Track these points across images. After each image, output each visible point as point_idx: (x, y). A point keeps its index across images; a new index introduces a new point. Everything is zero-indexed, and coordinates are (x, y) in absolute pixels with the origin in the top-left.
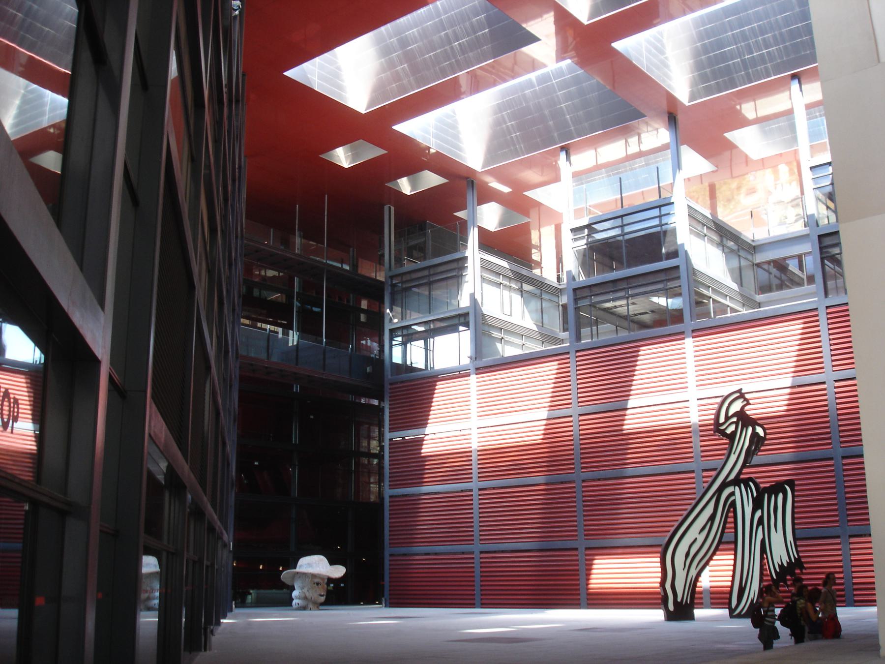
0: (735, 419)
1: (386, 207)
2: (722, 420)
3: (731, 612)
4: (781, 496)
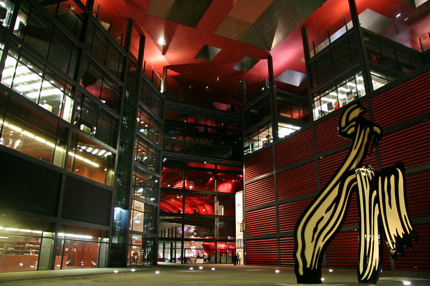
0: (354, 123)
2: (343, 124)
4: (393, 177)
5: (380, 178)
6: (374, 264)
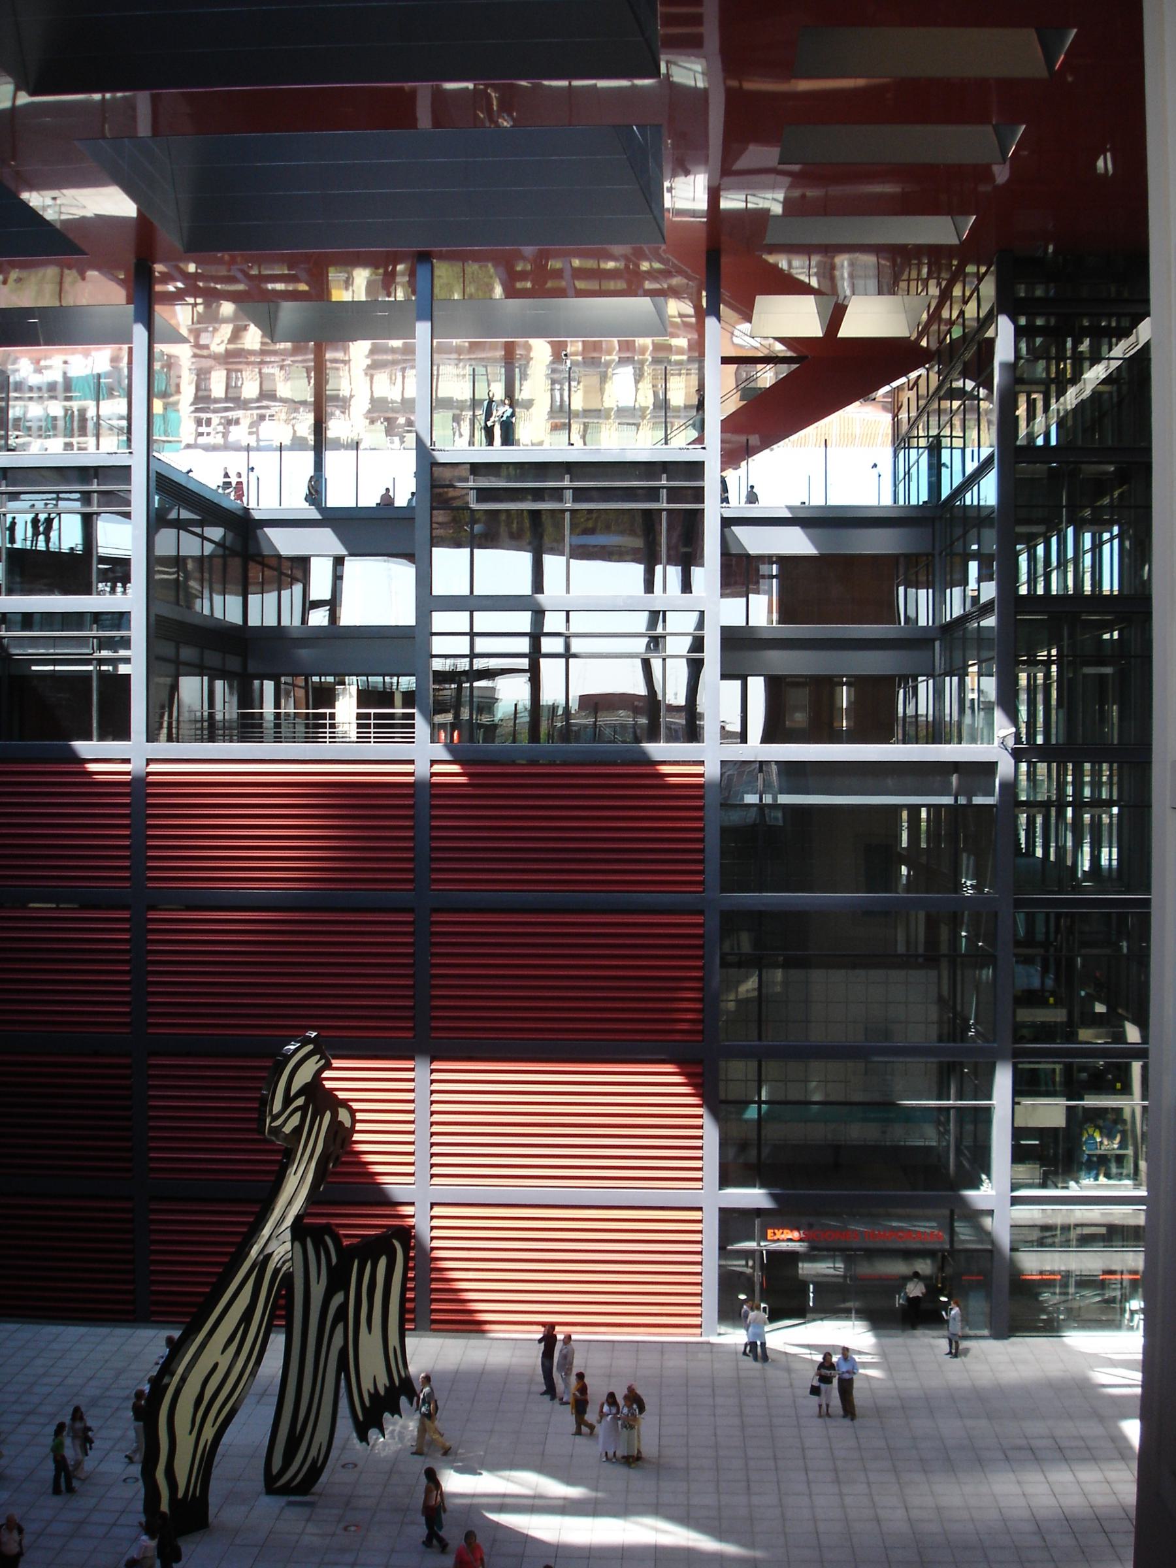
0: (300, 1101)
2: (277, 1106)
4: (383, 1262)
6: (313, 1452)
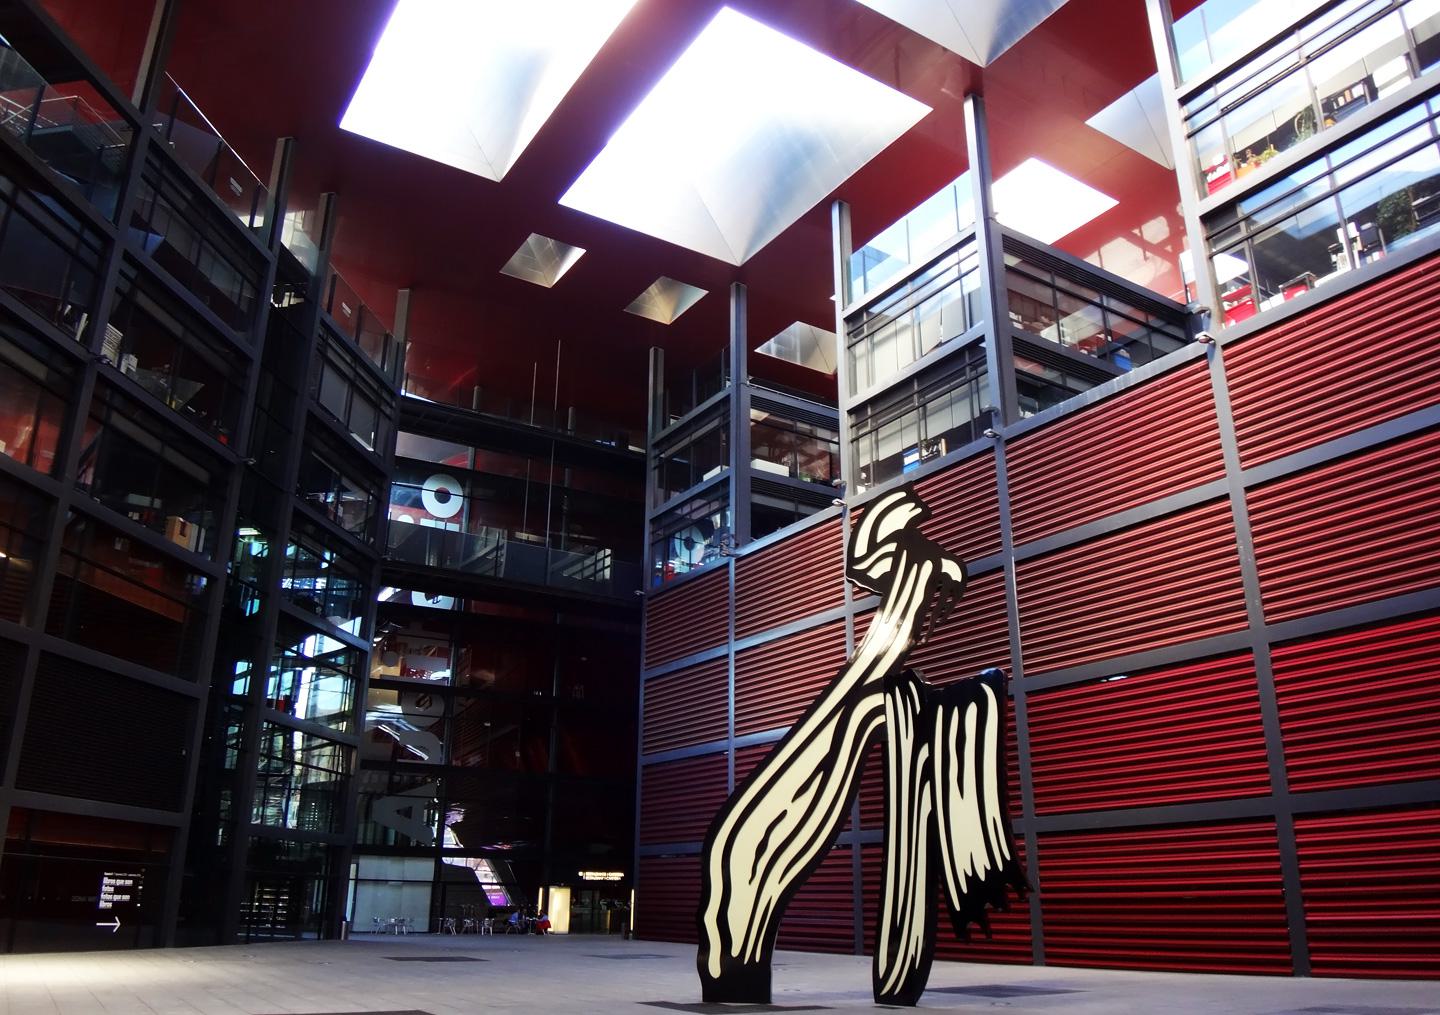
0: (892, 547)
1: (652, 350)
2: (861, 549)
3: (879, 983)
4: (972, 710)
5: (940, 708)
6: (911, 951)
